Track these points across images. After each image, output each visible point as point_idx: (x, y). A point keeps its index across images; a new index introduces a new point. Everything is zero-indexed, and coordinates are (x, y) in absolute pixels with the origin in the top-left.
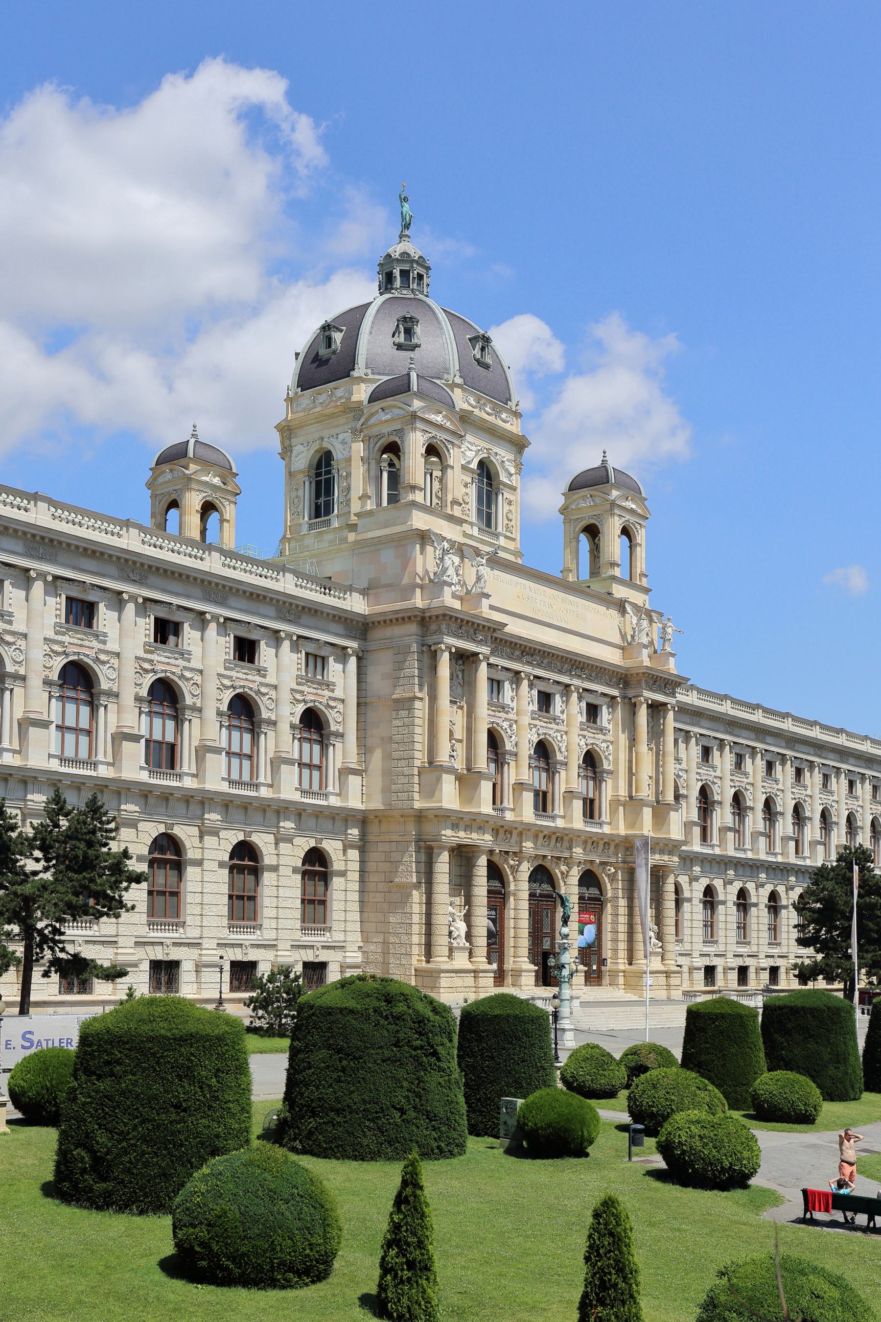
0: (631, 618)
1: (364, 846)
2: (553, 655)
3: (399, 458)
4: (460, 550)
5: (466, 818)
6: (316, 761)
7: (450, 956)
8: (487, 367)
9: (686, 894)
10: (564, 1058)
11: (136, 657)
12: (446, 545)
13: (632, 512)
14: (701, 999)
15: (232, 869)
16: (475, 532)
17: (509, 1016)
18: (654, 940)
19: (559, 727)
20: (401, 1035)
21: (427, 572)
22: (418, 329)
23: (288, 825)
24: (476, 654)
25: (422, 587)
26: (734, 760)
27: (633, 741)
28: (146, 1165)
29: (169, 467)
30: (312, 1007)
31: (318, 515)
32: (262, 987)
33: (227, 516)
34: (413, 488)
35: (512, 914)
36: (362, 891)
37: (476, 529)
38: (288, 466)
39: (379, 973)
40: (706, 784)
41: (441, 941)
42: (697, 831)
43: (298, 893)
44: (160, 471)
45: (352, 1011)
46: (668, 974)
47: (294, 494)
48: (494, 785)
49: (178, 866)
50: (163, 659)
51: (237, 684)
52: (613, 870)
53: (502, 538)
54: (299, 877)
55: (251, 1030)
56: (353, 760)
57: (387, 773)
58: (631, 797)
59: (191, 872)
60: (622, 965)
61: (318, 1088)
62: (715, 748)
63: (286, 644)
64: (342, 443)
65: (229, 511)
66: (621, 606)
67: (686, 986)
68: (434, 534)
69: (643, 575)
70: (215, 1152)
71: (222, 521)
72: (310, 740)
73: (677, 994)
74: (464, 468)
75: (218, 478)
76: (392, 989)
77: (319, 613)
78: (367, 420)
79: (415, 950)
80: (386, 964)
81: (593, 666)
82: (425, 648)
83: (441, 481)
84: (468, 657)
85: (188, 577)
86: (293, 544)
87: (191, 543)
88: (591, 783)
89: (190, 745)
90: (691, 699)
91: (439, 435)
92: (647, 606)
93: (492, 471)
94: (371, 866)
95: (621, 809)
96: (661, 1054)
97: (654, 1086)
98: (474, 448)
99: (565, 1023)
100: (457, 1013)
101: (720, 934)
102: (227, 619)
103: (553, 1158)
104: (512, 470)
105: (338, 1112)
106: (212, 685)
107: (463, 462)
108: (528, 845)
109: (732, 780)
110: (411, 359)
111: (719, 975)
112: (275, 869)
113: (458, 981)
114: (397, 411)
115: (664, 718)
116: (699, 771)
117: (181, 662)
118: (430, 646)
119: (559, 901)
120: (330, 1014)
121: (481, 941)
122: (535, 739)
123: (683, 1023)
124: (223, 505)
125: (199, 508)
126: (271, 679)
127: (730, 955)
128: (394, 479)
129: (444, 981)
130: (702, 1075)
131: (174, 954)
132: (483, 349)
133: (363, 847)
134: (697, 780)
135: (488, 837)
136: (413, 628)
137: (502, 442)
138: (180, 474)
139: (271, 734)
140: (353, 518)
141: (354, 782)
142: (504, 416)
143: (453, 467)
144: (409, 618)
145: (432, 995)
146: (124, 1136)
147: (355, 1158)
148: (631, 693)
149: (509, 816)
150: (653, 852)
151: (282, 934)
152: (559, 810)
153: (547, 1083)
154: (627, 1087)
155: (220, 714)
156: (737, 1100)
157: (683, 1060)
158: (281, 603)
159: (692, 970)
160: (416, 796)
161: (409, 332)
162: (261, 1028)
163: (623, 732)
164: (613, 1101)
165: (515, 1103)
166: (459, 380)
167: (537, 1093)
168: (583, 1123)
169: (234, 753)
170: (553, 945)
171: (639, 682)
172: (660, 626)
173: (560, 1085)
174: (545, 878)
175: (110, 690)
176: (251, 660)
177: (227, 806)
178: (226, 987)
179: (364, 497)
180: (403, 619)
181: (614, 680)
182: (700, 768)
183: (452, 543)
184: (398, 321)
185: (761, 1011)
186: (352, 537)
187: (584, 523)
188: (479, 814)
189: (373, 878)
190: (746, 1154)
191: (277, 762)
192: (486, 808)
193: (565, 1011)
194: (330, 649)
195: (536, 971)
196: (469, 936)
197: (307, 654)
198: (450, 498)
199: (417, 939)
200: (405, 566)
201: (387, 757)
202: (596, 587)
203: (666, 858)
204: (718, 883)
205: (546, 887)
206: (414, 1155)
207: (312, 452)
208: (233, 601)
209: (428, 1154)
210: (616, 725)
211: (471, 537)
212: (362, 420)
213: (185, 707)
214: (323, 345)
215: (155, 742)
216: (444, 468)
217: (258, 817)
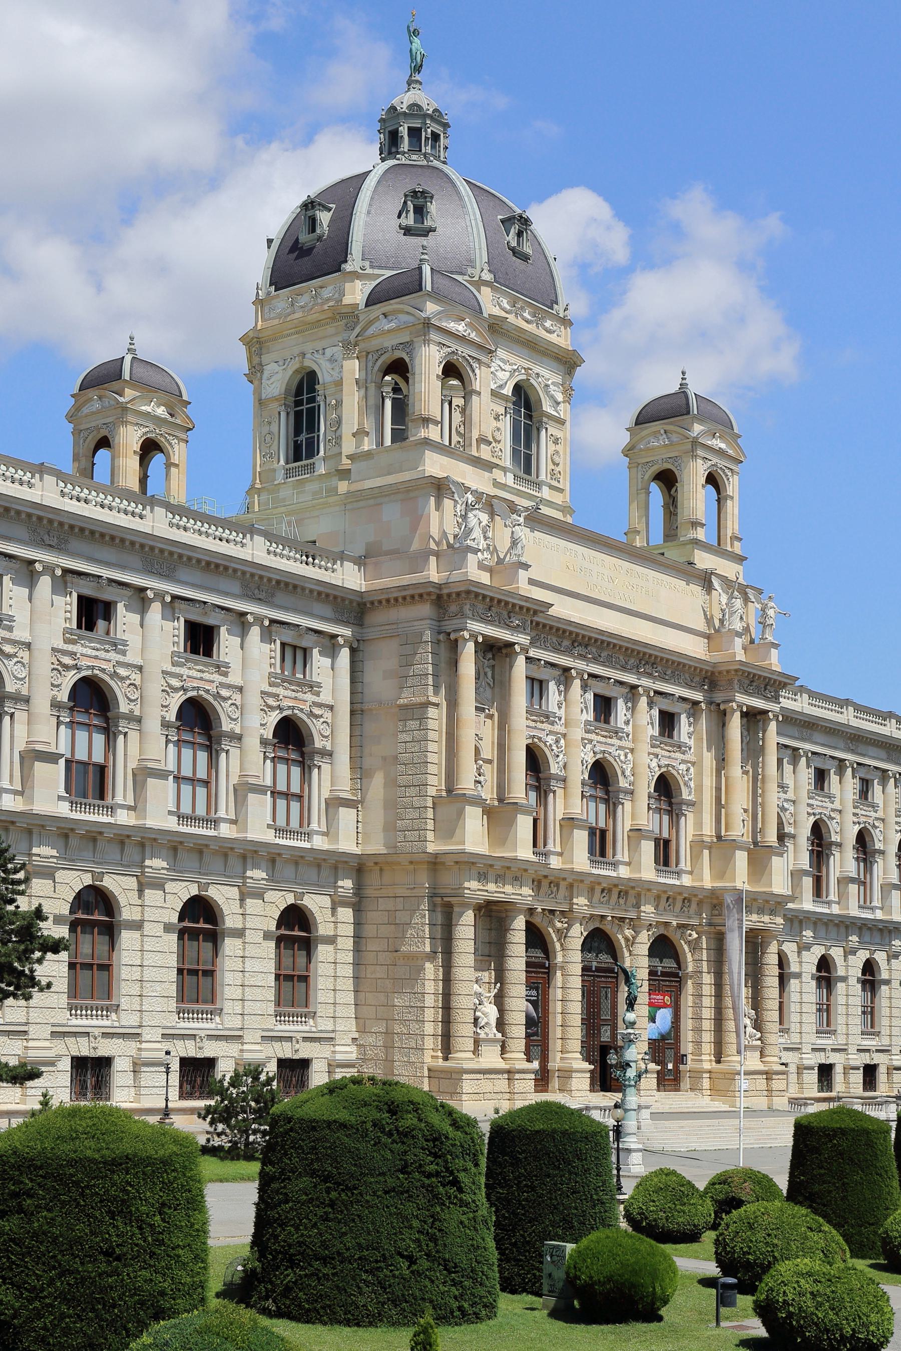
0: (720, 596)
1: (360, 902)
2: (615, 645)
3: (407, 380)
4: (489, 505)
5: (498, 865)
6: (295, 789)
7: (476, 1051)
8: (525, 258)
9: (794, 968)
10: (628, 1188)
11: (53, 649)
12: (470, 498)
13: (721, 453)
14: (813, 1109)
15: (182, 933)
16: (510, 480)
17: (554, 1131)
18: (750, 1030)
19: (623, 743)
20: (410, 1158)
21: (445, 534)
22: (433, 207)
23: (257, 875)
24: (511, 645)
25: (437, 554)
26: (858, 787)
27: (722, 762)
28: (66, 1332)
29: (97, 392)
30: (289, 1120)
31: (297, 458)
32: (222, 1093)
33: (175, 459)
34: (426, 421)
35: (559, 994)
36: (356, 964)
37: (510, 476)
38: (258, 392)
39: (379, 1074)
40: (821, 819)
41: (463, 1030)
42: (808, 883)
43: (271, 967)
44: (84, 398)
45: (343, 1126)
46: (769, 1075)
47: (265, 429)
48: (535, 821)
49: (110, 931)
50: (90, 652)
51: (189, 684)
52: (695, 935)
53: (545, 489)
54: (272, 944)
55: (209, 1150)
56: (345, 787)
57: (391, 805)
58: (719, 837)
59: (127, 938)
60: (708, 1063)
61: (297, 1229)
62: (832, 772)
63: (255, 631)
64: (330, 360)
65: (178, 452)
66: (706, 580)
67: (793, 1092)
68: (454, 482)
69: (735, 538)
70: (160, 1314)
71: (169, 465)
72: (286, 761)
73: (781, 1102)
74: (495, 394)
75: (163, 408)
76: (398, 1096)
77: (299, 590)
78: (364, 329)
79: (429, 1043)
80: (389, 1061)
81: (668, 660)
82: (441, 637)
83: (463, 411)
84: (500, 649)
85: (123, 540)
86: (264, 497)
87: (126, 495)
88: (666, 818)
89: (125, 767)
90: (801, 705)
91: (460, 349)
92: (741, 580)
93: (533, 399)
94: (369, 930)
95: (706, 852)
96: (759, 1183)
97: (751, 1227)
98: (507, 367)
99: (630, 1142)
100: (485, 1128)
101: (840, 1021)
102: (175, 597)
103: (614, 1323)
104: (560, 397)
105: (325, 1260)
106: (155, 687)
107: (493, 387)
108: (581, 901)
109: (855, 814)
110: (424, 247)
111: (838, 1076)
112: (240, 933)
113: (486, 1085)
114: (404, 318)
115: (764, 731)
116: (811, 802)
117: (113, 656)
118: (449, 634)
119: (622, 977)
120: (314, 1129)
121: (518, 1031)
122: (591, 759)
123: (790, 1142)
124: (170, 444)
125: (137, 447)
126: (234, 678)
127: (852, 1049)
128: (401, 409)
129: (468, 1085)
130: (815, 1212)
131: (104, 1049)
132: (520, 234)
133: (359, 903)
134: (808, 813)
135: (527, 891)
136: (426, 609)
137: (545, 359)
138: (112, 402)
139: (234, 752)
140: (345, 461)
141: (347, 816)
142: (548, 324)
143: (479, 393)
144: (421, 596)
145: (451, 1103)
146: (36, 1293)
147: (348, 1323)
148: (719, 697)
149: (555, 862)
150: (749, 911)
151: (249, 1022)
152: (622, 854)
153: (606, 1222)
154: (715, 1227)
155: (165, 725)
156: (862, 1246)
157: (789, 1190)
158: (248, 575)
159: (801, 1069)
160: (430, 836)
161: (420, 211)
162: (220, 1148)
163: (709, 750)
164: (695, 1246)
165: (563, 1249)
166: (487, 276)
167: (594, 1235)
168: (655, 1275)
169: (184, 778)
170: (614, 1035)
171: (730, 682)
172: (759, 606)
173: (623, 1224)
174: (603, 946)
175: (18, 692)
176: (208, 653)
177: (175, 849)
178: (174, 1093)
179: (360, 433)
180: (413, 597)
181: (697, 679)
182: (812, 798)
183: (478, 495)
184: (406, 196)
185: (894, 1125)
186: (343, 487)
187: (656, 469)
188: (515, 859)
189: (372, 946)
190: (874, 1318)
191: (243, 790)
192: (525, 852)
193: (630, 1125)
194: (314, 637)
195: (592, 1072)
196: (501, 1024)
197: (283, 645)
198: (475, 435)
199: (431, 1028)
200: (414, 528)
201: (391, 783)
202: (673, 554)
203: (766, 919)
204: (836, 953)
205: (605, 959)
206: (428, 1318)
207: (290, 372)
208: (183, 573)
209: (445, 1318)
210: (699, 740)
211: (503, 487)
212: (358, 330)
213: (120, 716)
214: (305, 229)
215: (79, 762)
216: (468, 393)
217: (218, 864)
